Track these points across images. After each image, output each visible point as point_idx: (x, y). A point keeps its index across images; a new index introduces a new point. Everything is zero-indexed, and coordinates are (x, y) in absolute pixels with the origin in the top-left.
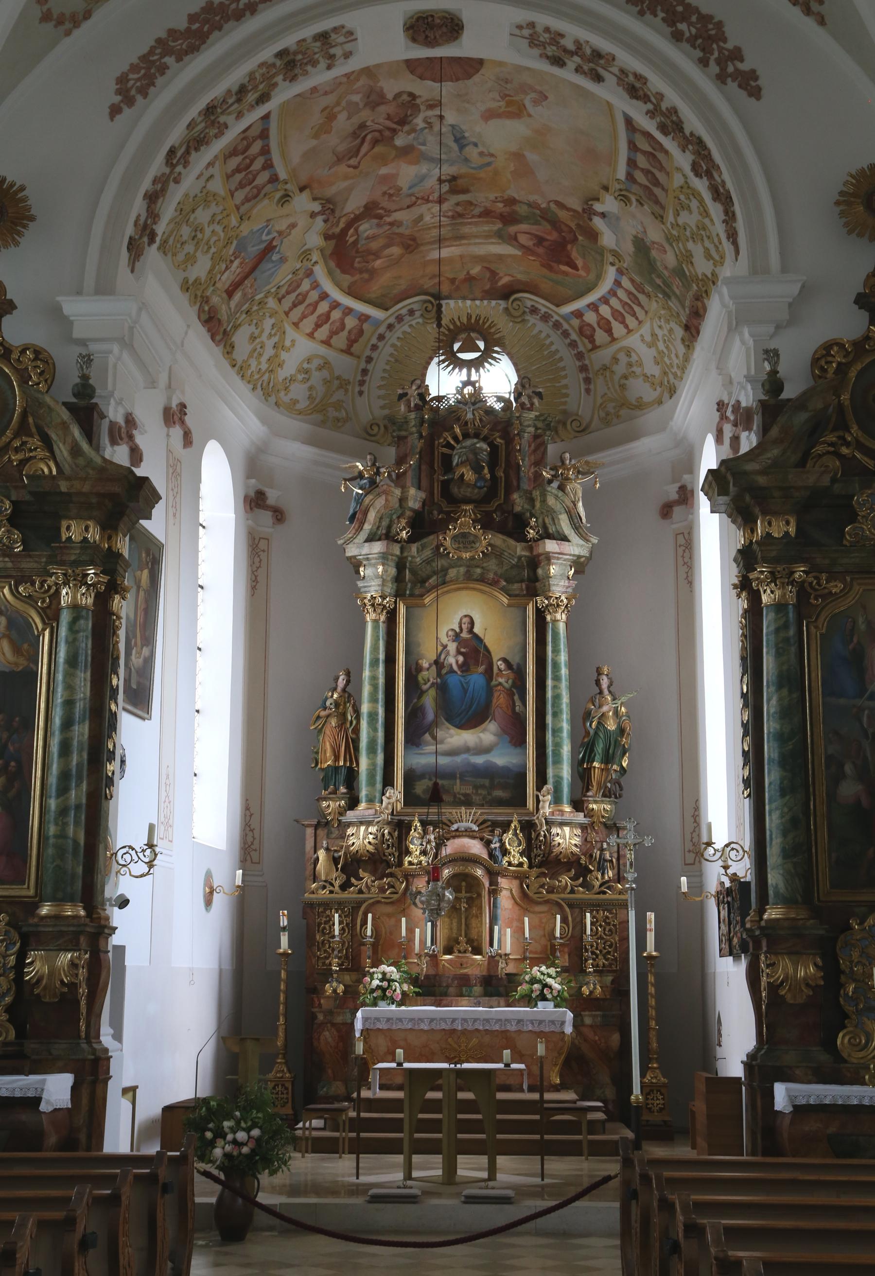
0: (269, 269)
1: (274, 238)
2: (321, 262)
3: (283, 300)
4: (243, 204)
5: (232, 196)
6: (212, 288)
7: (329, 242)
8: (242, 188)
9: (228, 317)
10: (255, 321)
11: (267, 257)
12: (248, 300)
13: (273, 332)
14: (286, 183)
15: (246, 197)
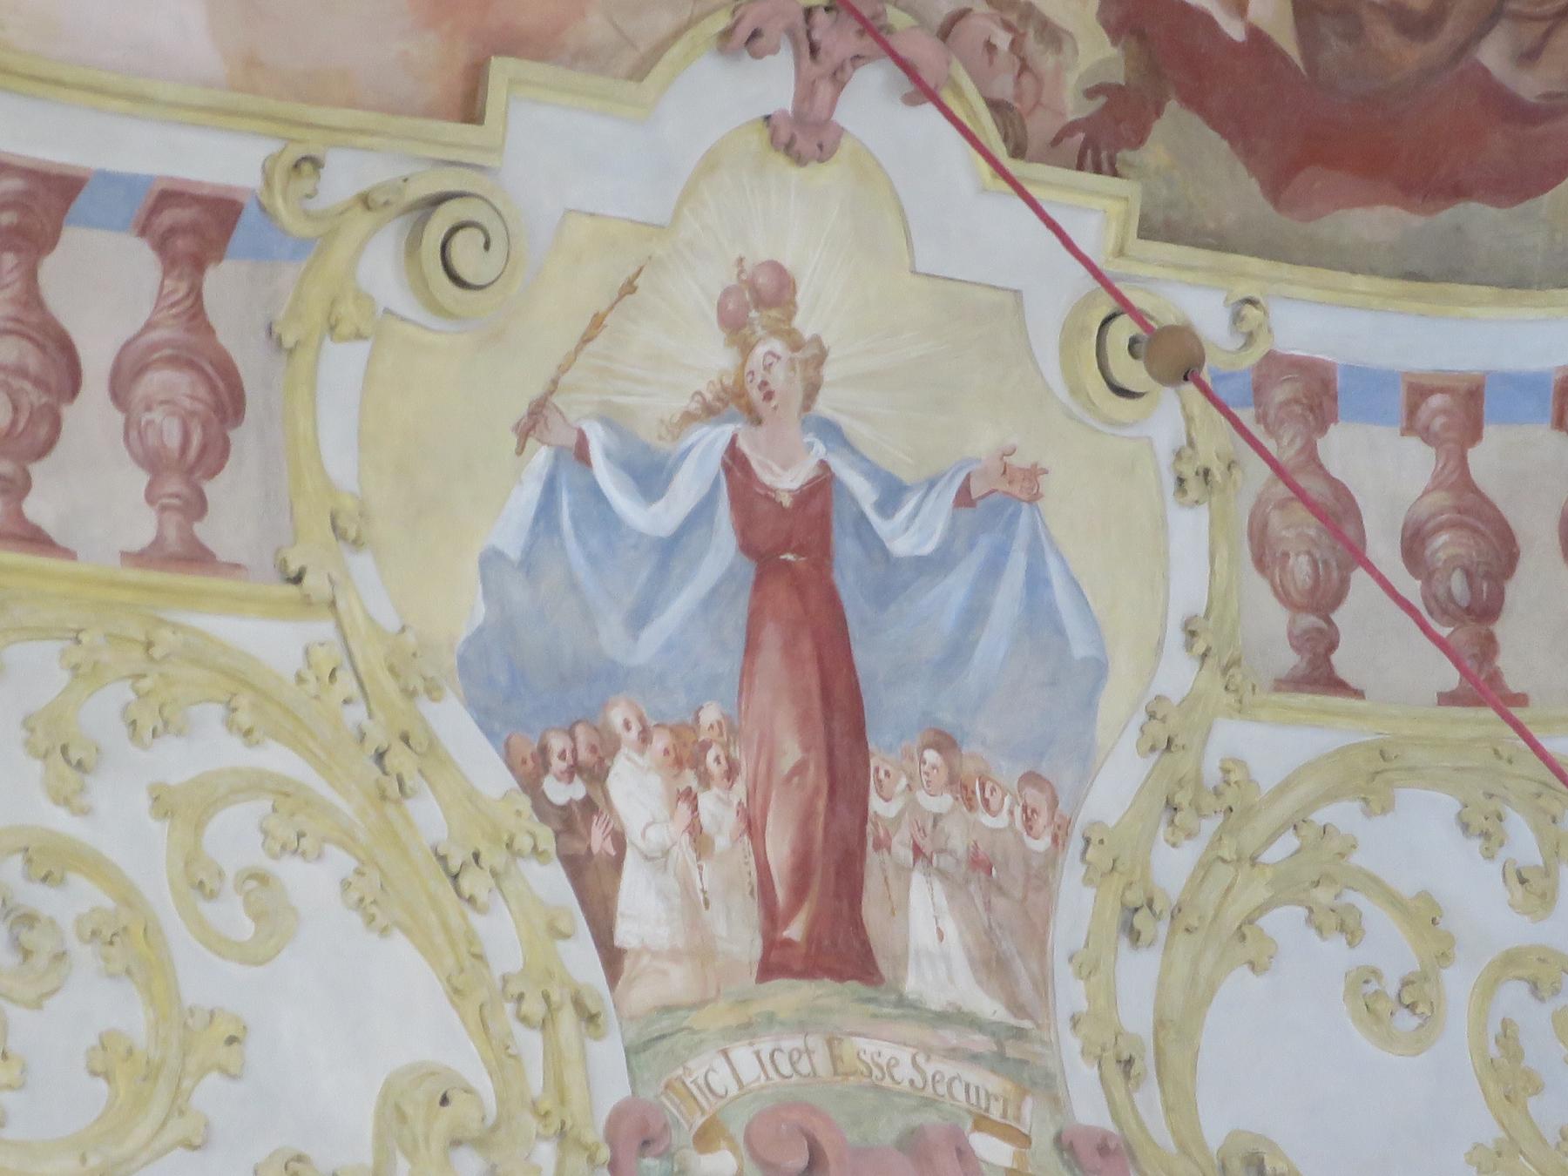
0: (975, 614)
1: (735, 461)
2: (1253, 274)
3: (1343, 662)
4: (197, 506)
5: (36, 540)
6: (608, 1054)
7: (1155, 152)
8: (44, 450)
9: (999, 1062)
10: (1284, 922)
11: (848, 578)
12: (1041, 878)
13: (1523, 842)
14: (309, 164)
15: (153, 462)
